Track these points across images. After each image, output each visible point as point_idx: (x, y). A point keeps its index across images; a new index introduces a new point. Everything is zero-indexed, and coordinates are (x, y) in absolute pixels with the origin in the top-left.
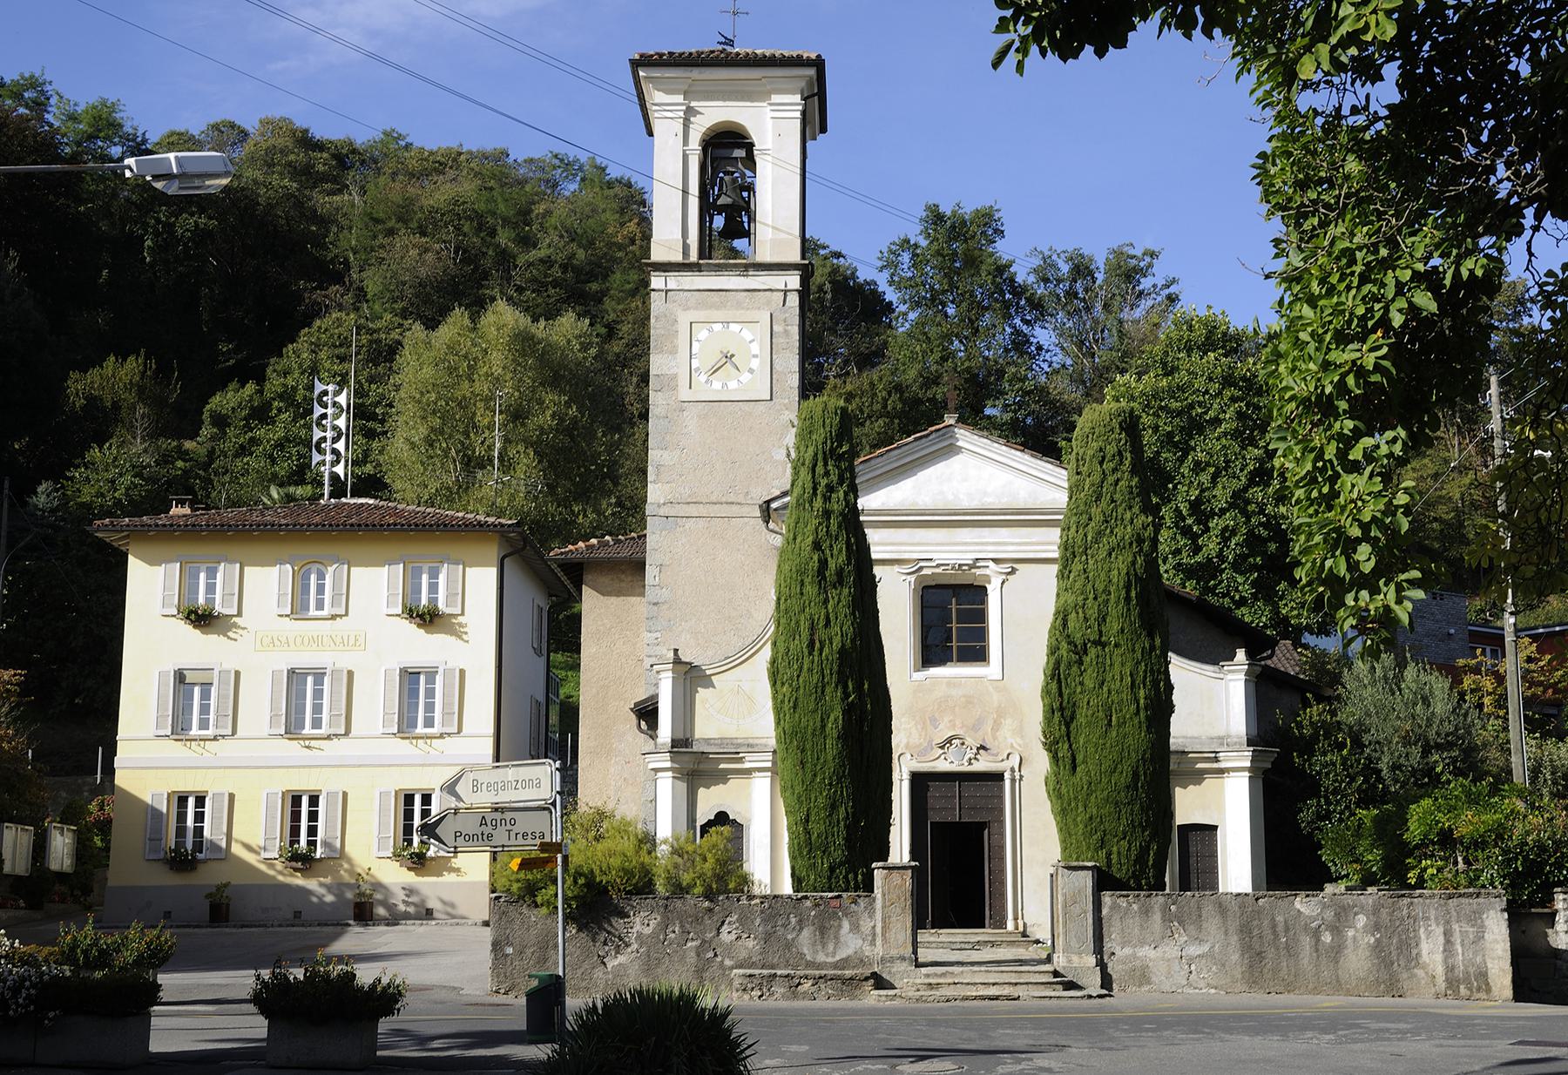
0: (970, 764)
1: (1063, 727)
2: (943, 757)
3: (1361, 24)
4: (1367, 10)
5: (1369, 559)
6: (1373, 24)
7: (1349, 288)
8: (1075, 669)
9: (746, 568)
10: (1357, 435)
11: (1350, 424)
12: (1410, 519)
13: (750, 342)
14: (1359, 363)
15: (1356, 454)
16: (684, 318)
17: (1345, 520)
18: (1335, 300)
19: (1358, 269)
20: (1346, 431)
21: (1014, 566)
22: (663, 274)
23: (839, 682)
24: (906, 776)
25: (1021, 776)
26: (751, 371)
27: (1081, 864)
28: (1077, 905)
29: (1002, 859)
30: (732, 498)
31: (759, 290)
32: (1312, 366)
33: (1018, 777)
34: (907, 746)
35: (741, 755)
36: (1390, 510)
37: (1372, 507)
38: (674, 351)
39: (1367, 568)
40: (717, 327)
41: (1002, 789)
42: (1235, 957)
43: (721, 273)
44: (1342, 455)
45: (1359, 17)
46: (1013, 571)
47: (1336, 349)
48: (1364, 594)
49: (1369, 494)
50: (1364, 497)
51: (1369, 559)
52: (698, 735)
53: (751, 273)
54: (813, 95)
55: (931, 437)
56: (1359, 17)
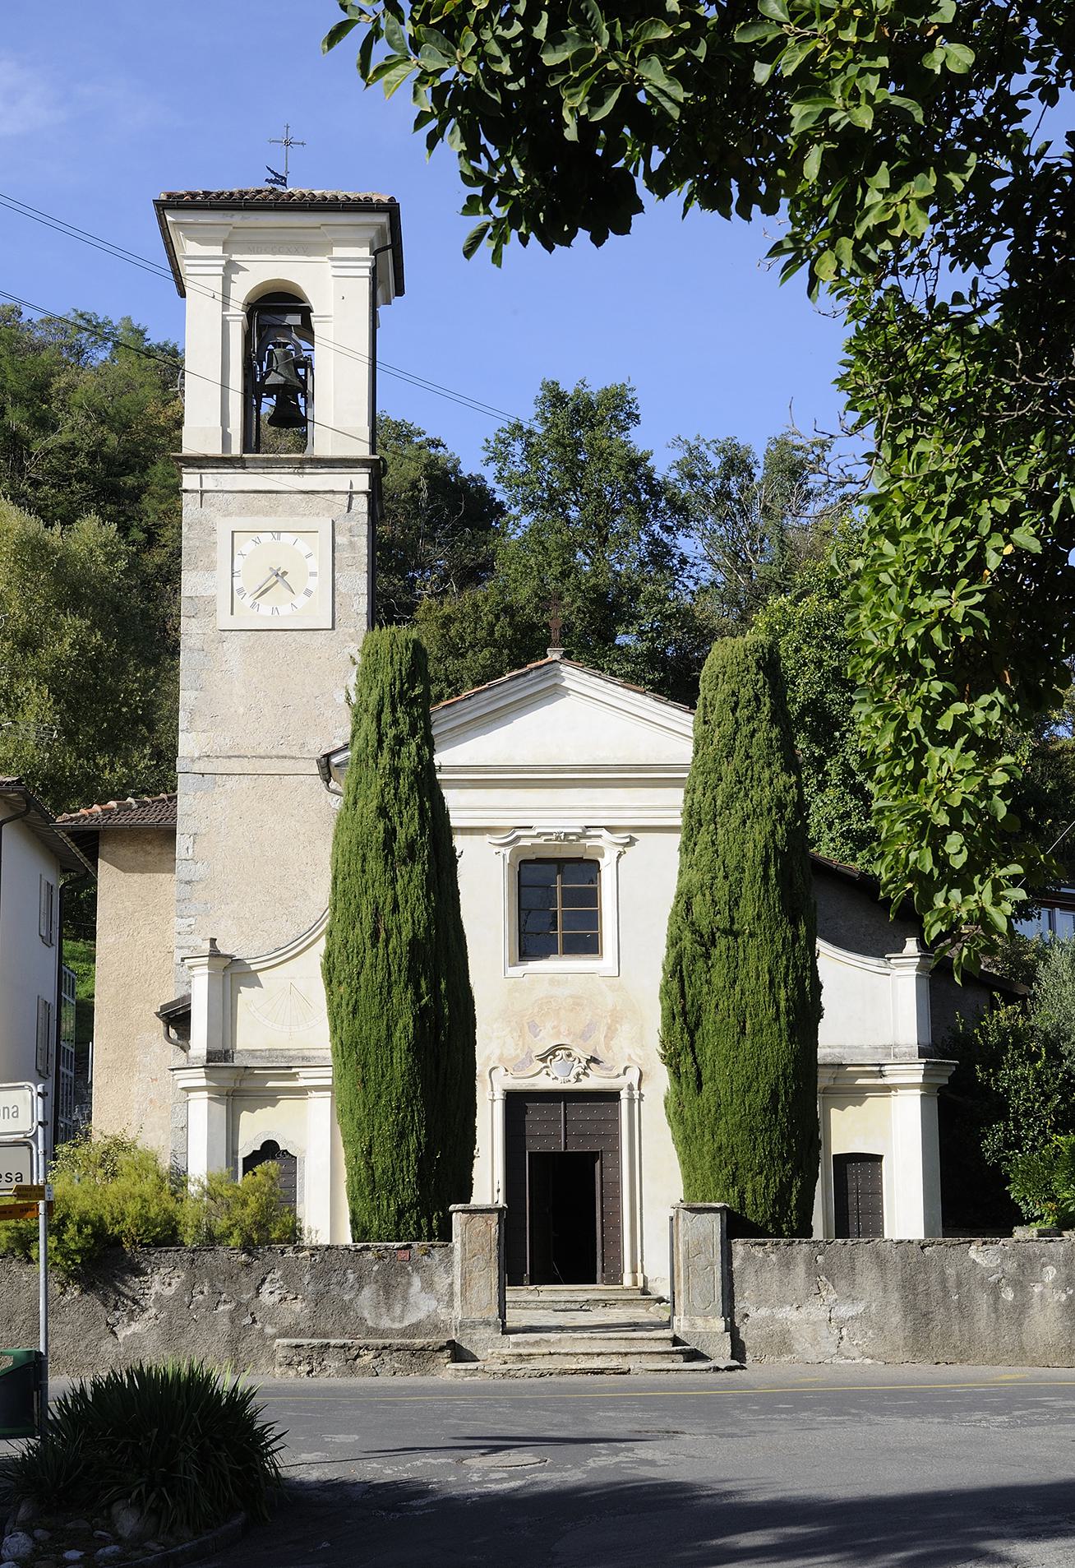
0: (578, 1080)
1: (686, 1036)
2: (544, 1071)
3: (889, 216)
4: (896, 198)
5: (960, 852)
6: (903, 216)
7: (936, 520)
8: (700, 964)
9: (301, 837)
10: (947, 699)
11: (938, 686)
12: (1008, 802)
13: (307, 557)
14: (946, 613)
15: (945, 723)
16: (224, 526)
17: (930, 804)
18: (920, 535)
19: (946, 498)
20: (934, 695)
21: (632, 835)
22: (197, 471)
23: (409, 980)
24: (499, 1096)
25: (641, 1096)
26: (308, 593)
27: (707, 1204)
28: (702, 1256)
29: (618, 1197)
30: (284, 751)
31: (318, 492)
32: (893, 616)
33: (637, 1096)
34: (500, 1059)
35: (294, 1070)
36: (986, 790)
37: (963, 789)
38: (211, 568)
39: (958, 862)
40: (266, 538)
41: (617, 1111)
42: (896, 1319)
43: (270, 470)
44: (929, 723)
45: (888, 206)
46: (632, 842)
47: (922, 594)
48: (956, 894)
49: (961, 772)
50: (955, 776)
51: (960, 852)
52: (241, 1044)
53: (307, 471)
54: (385, 249)
55: (530, 676)
56: (888, 206)
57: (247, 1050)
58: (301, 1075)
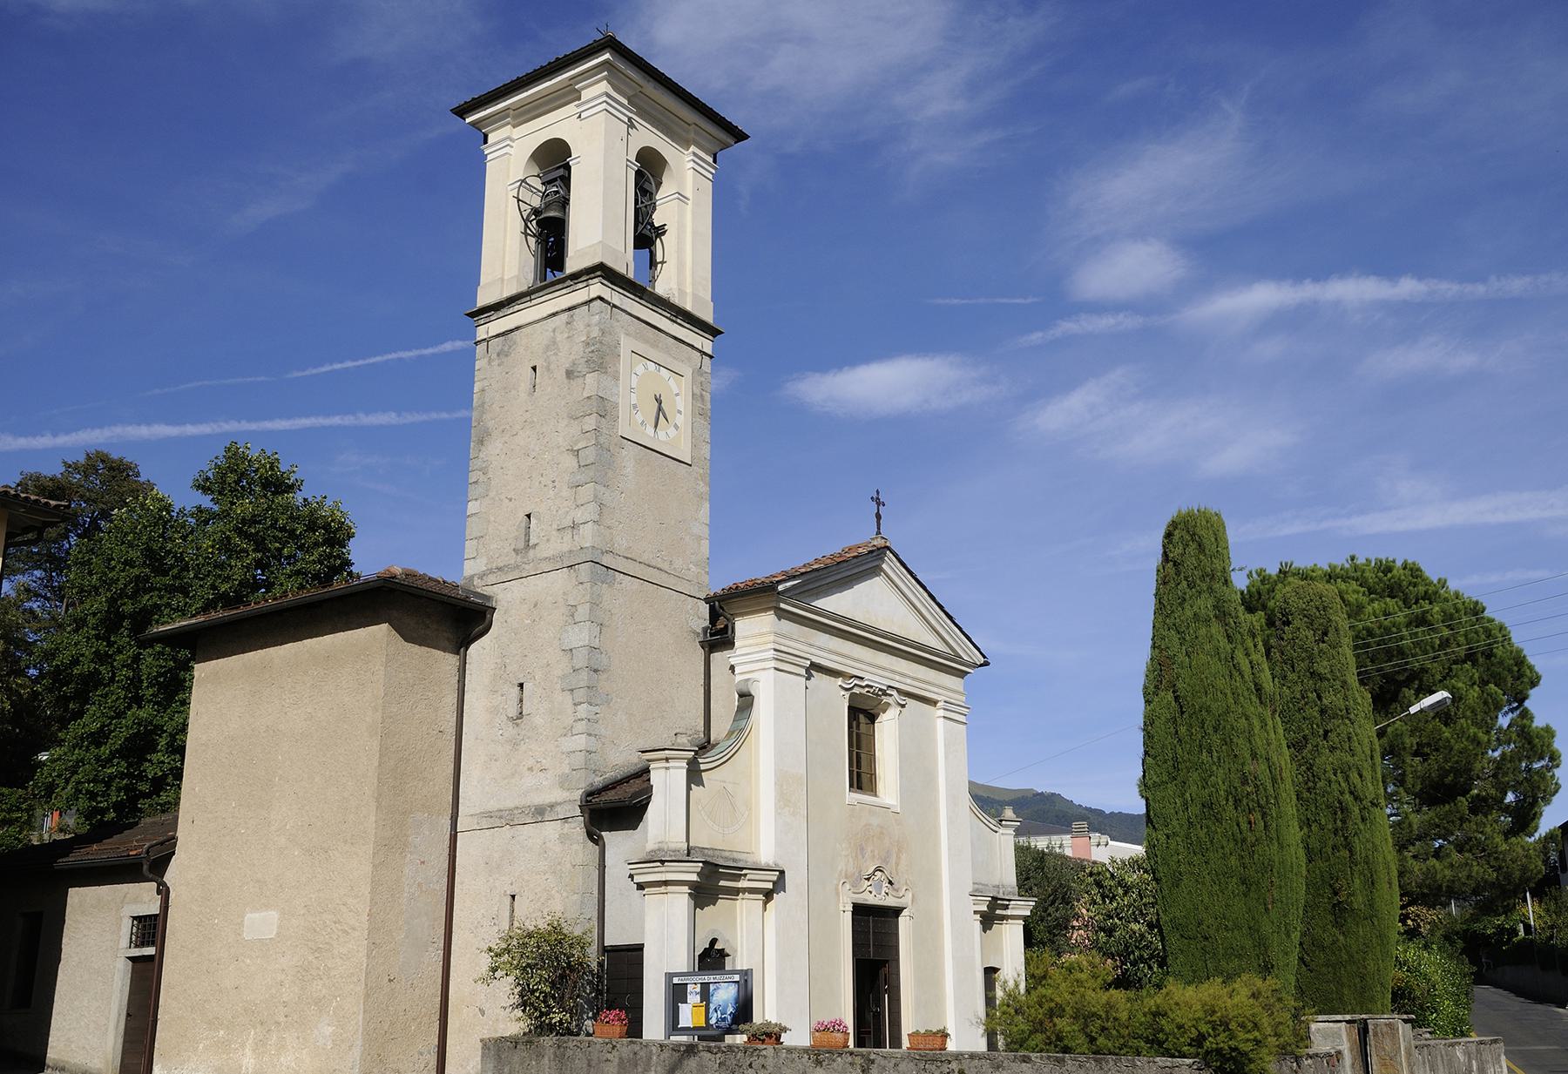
16: (626, 344)
22: (610, 285)
26: (676, 427)
31: (683, 342)
53: (679, 321)
55: (875, 554)
57: (699, 847)
58: (747, 877)
